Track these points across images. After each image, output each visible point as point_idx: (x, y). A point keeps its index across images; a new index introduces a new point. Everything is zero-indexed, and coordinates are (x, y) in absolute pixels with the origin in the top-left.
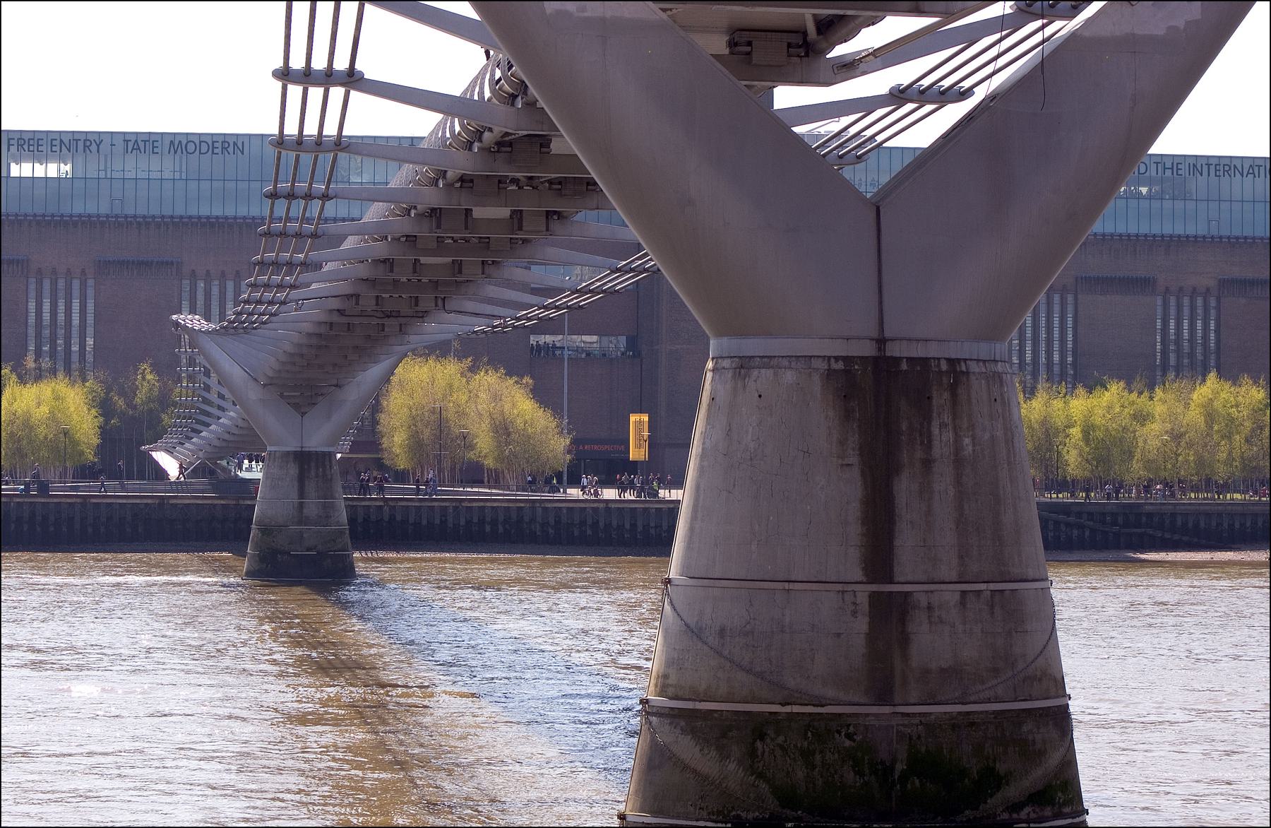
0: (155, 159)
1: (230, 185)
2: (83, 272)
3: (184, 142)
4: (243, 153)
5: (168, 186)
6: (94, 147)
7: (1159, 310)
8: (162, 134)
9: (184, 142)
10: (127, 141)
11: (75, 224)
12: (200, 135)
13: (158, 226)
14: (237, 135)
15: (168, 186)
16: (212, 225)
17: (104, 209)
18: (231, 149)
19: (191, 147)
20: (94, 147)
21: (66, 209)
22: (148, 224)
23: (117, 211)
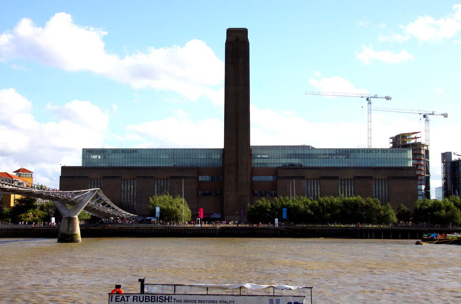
0: (118, 154)
1: (135, 160)
2: (100, 179)
3: (125, 151)
4: (137, 152)
5: (116, 160)
6: (105, 152)
7: (340, 184)
8: (120, 149)
9: (125, 151)
10: (112, 151)
11: (99, 168)
12: (128, 149)
13: (117, 169)
14: (136, 149)
15: (121, 160)
16: (128, 168)
17: (107, 165)
18: (135, 152)
19: (126, 152)
20: (105, 152)
21: (99, 165)
22: (114, 168)
23: (110, 166)
